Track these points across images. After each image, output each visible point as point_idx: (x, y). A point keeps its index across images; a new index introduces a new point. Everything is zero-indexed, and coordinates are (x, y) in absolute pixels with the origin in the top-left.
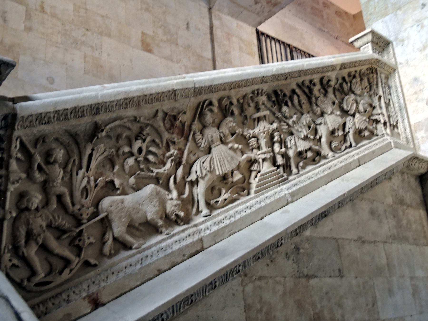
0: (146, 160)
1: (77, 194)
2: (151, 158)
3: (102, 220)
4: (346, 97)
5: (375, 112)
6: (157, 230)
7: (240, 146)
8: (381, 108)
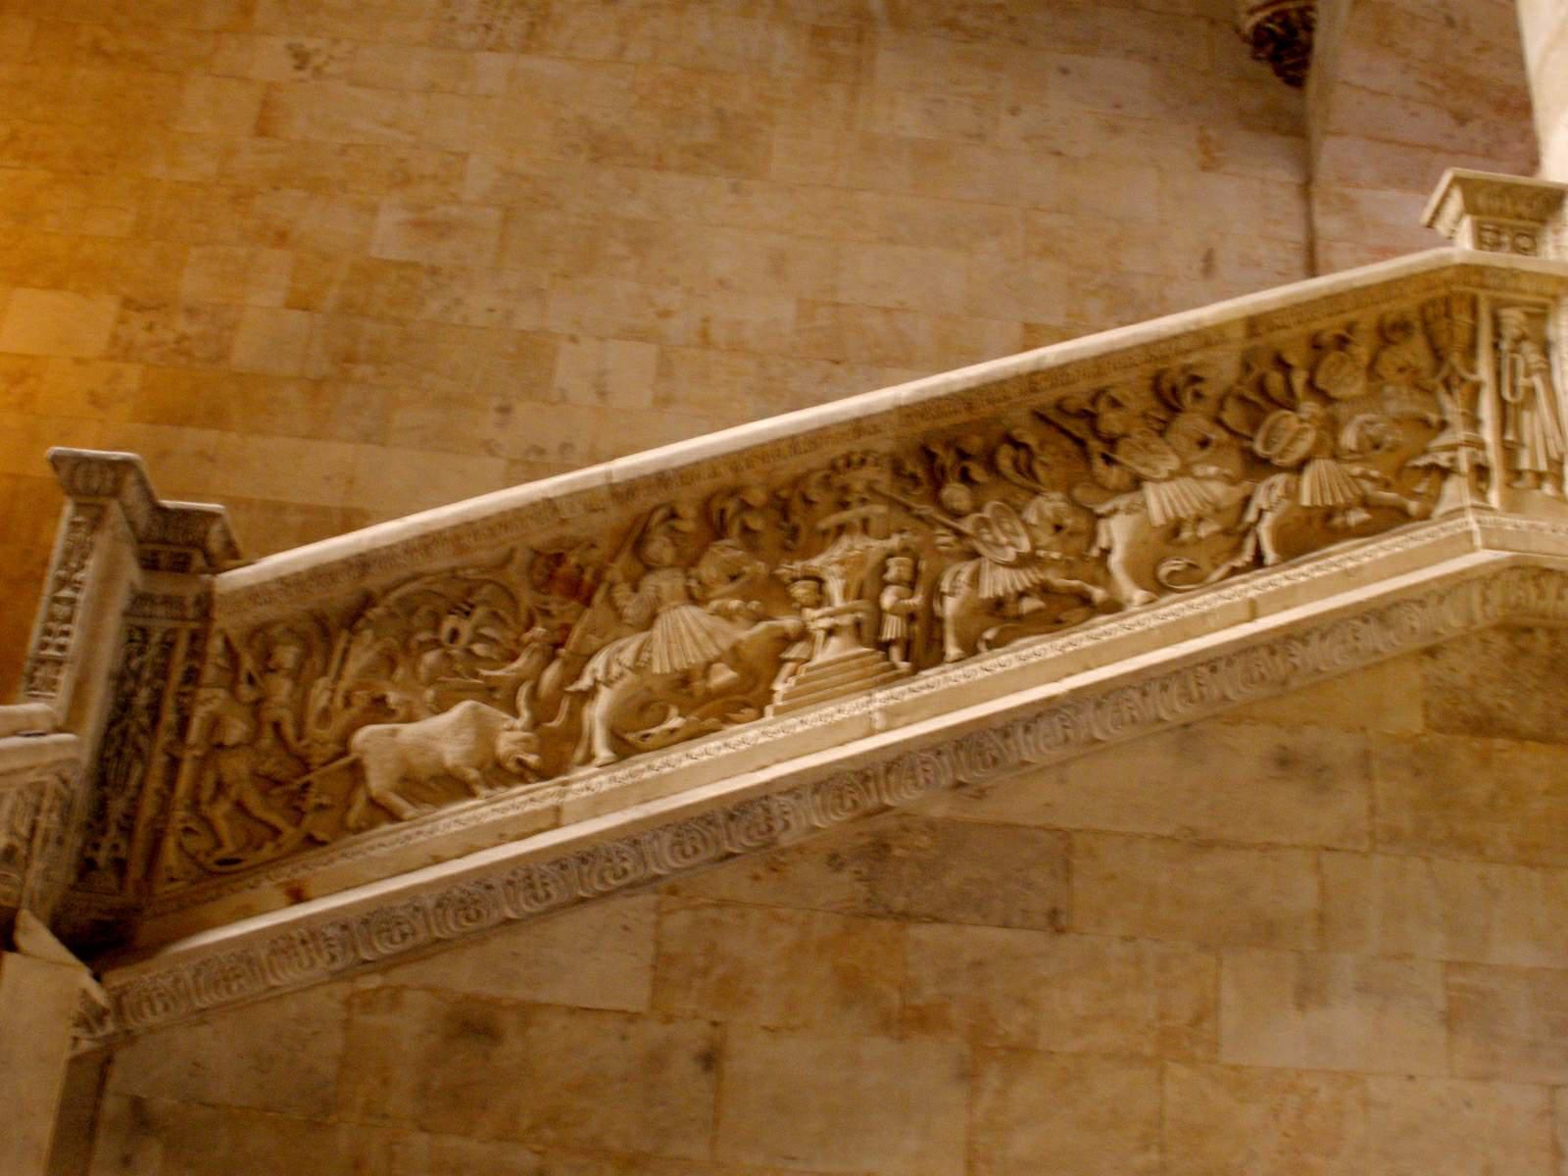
1: (311, 720)
2: (479, 649)
8: (1475, 423)
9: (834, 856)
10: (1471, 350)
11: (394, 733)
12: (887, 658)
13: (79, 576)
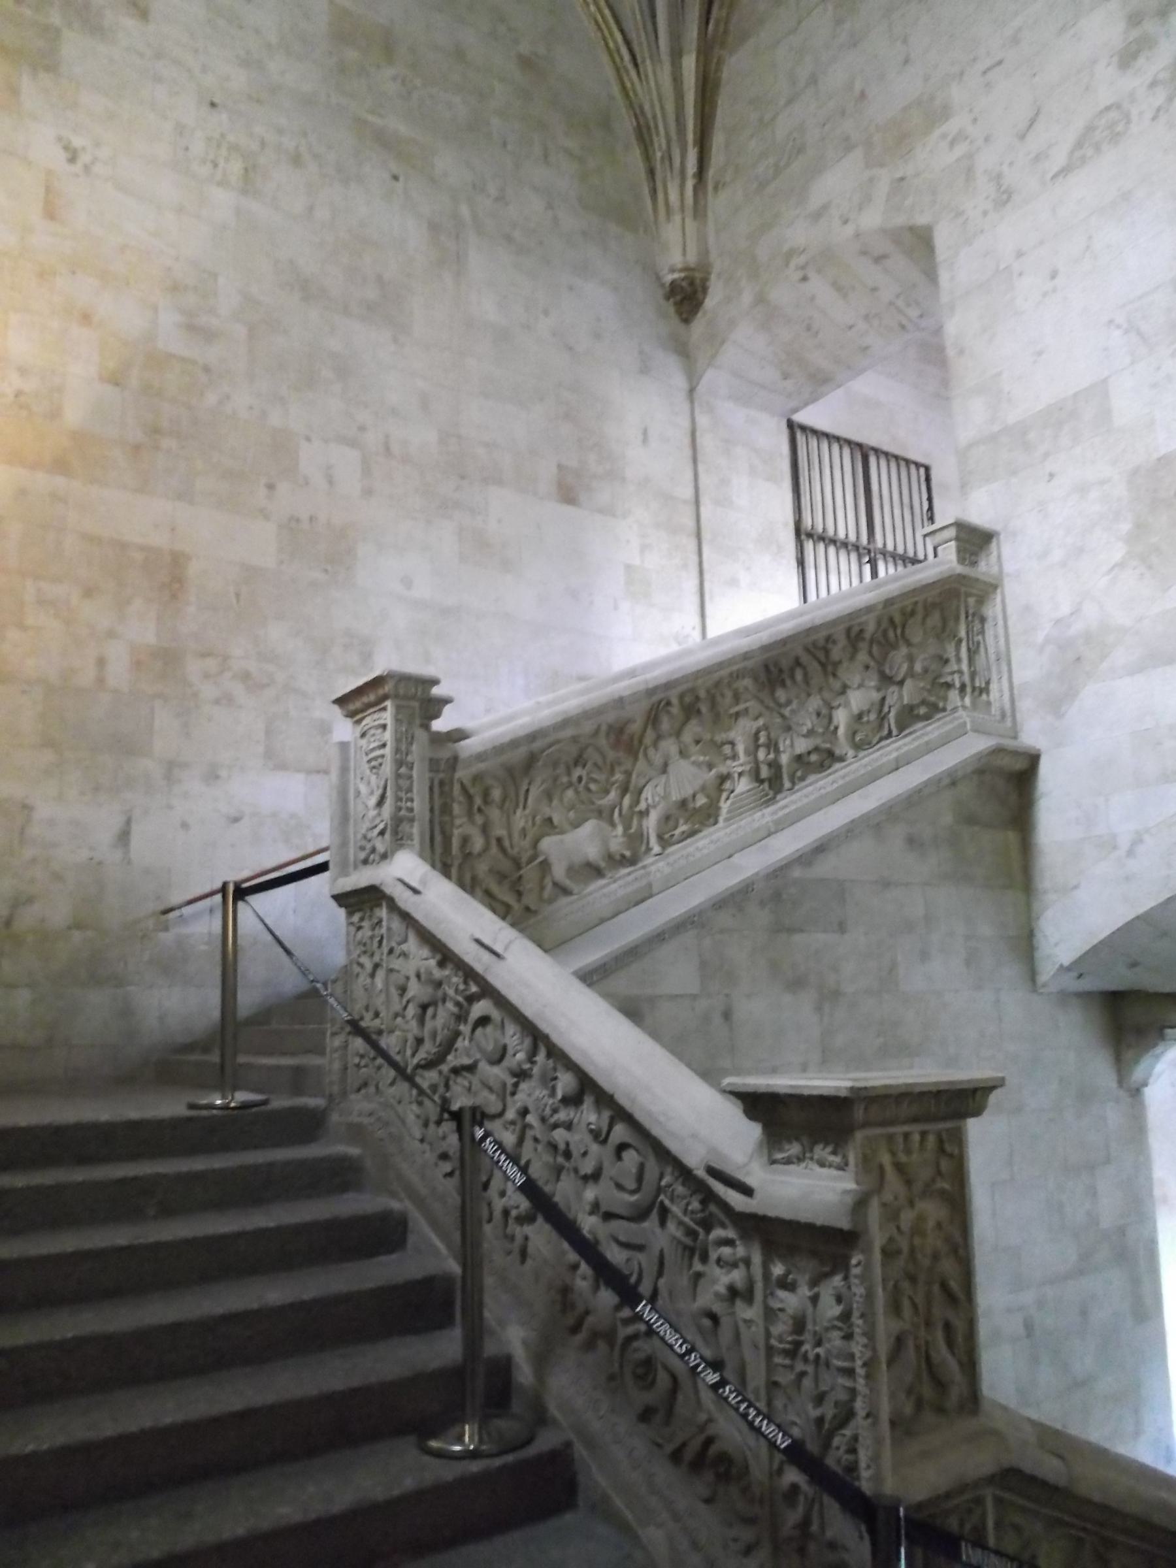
0: (589, 790)
1: (516, 835)
2: (593, 786)
3: (541, 863)
4: (893, 653)
5: (948, 669)
7: (707, 758)
8: (959, 660)
10: (957, 619)
13: (409, 758)
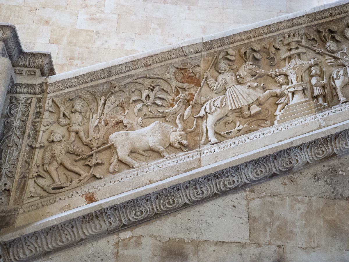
6: (159, 154)
9: (316, 175)
11: (127, 134)
12: (318, 101)
